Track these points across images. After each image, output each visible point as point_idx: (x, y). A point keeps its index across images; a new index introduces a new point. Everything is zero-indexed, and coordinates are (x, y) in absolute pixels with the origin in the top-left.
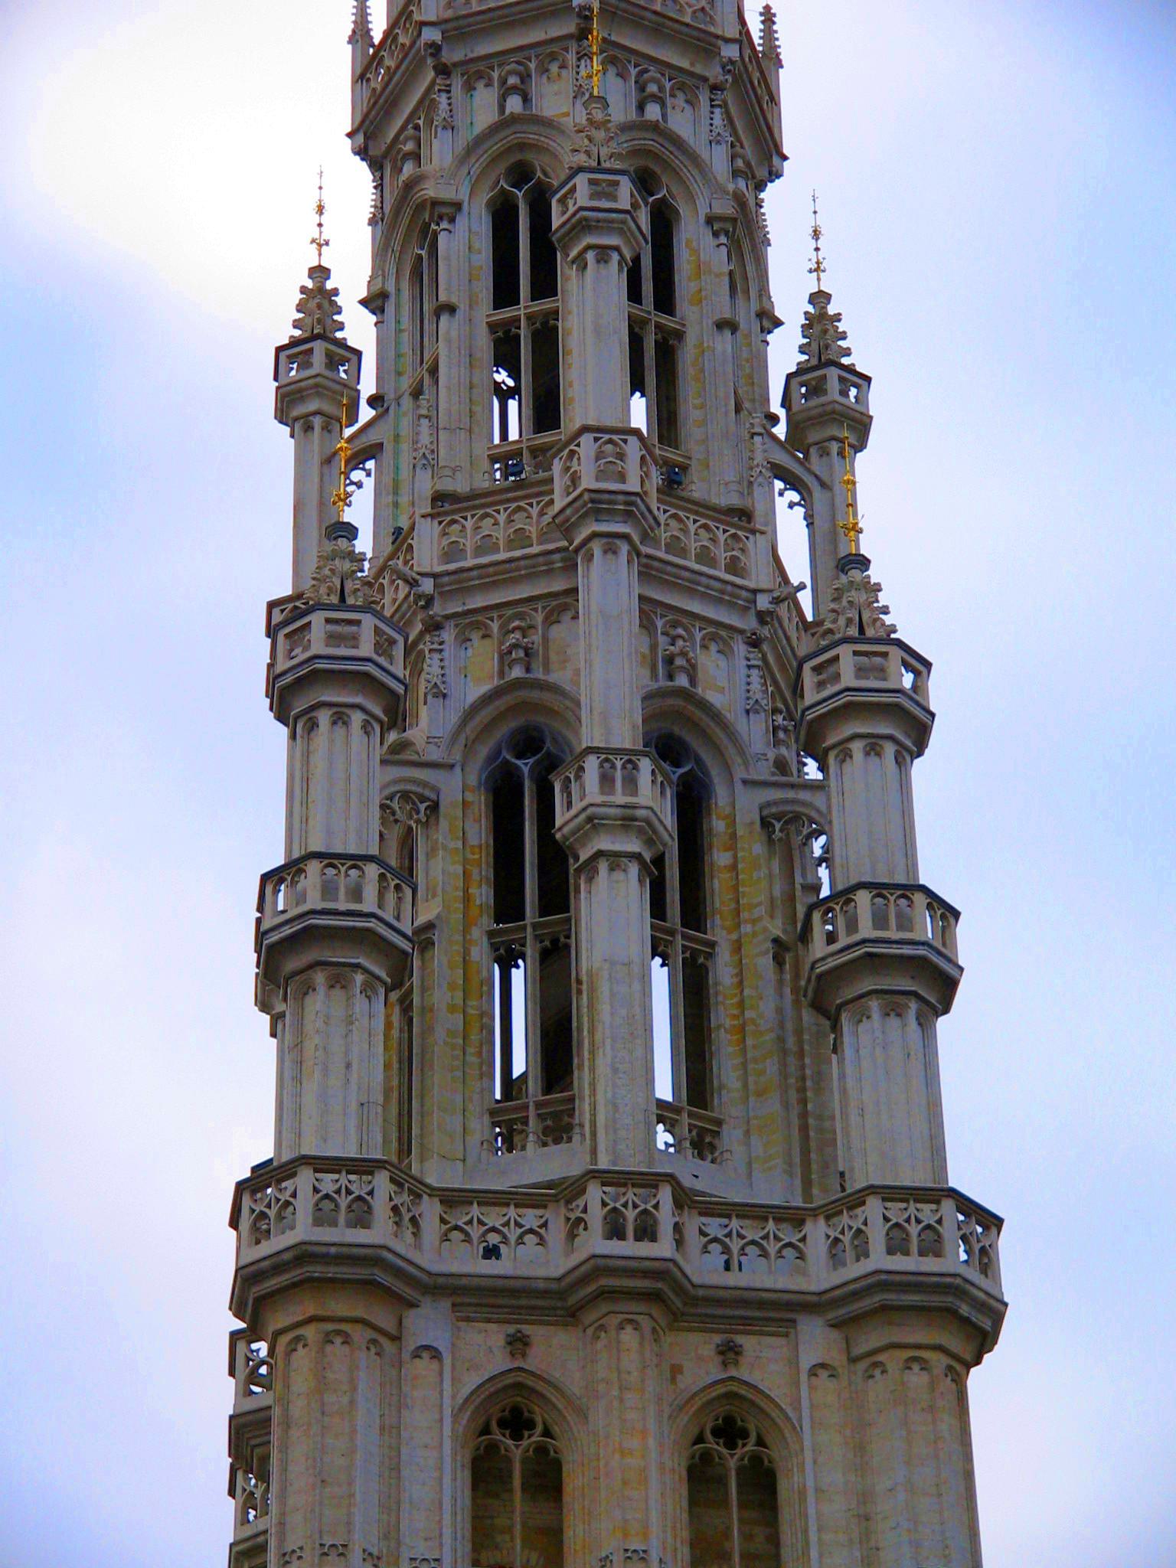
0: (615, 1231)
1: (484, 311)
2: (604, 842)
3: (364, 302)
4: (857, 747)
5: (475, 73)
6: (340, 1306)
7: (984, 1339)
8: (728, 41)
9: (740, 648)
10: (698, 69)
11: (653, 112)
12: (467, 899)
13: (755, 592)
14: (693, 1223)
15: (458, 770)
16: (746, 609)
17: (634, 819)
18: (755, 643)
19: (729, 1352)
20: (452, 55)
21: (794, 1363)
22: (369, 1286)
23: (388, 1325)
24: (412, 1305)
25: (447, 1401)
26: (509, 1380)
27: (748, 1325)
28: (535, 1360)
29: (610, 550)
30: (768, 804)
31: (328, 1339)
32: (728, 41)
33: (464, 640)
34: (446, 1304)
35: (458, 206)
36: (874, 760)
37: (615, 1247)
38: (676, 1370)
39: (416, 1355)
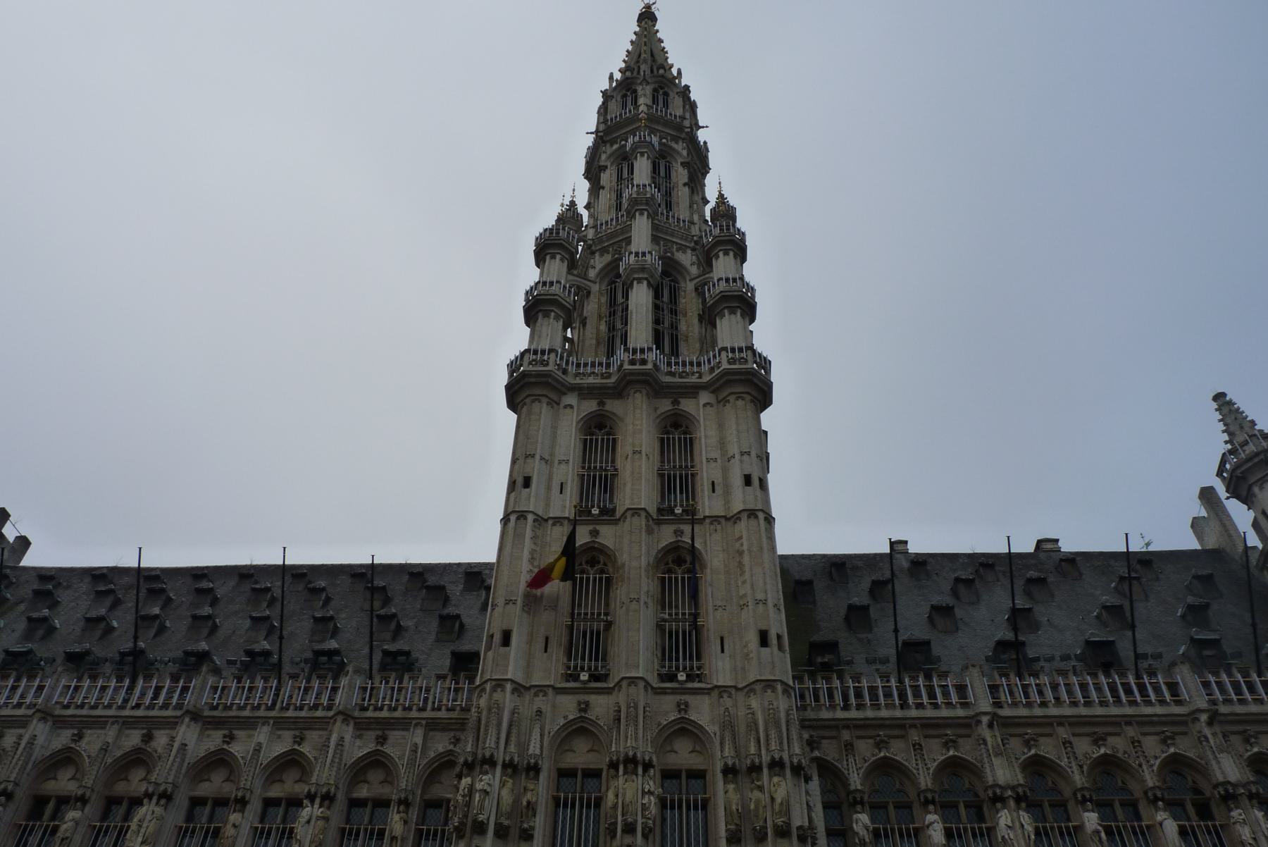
2: (636, 276)
3: (585, 207)
4: (721, 254)
6: (538, 391)
7: (763, 397)
8: (687, 128)
9: (689, 251)
10: (678, 135)
11: (664, 141)
13: (693, 236)
15: (598, 284)
16: (691, 241)
17: (645, 268)
18: (693, 249)
19: (676, 402)
21: (698, 405)
22: (547, 385)
23: (555, 398)
24: (565, 394)
25: (575, 418)
26: (598, 412)
29: (642, 214)
30: (697, 283)
31: (533, 401)
32: (687, 128)
33: (602, 255)
34: (576, 393)
35: (606, 167)
36: (726, 257)
38: (656, 409)
39: (565, 407)
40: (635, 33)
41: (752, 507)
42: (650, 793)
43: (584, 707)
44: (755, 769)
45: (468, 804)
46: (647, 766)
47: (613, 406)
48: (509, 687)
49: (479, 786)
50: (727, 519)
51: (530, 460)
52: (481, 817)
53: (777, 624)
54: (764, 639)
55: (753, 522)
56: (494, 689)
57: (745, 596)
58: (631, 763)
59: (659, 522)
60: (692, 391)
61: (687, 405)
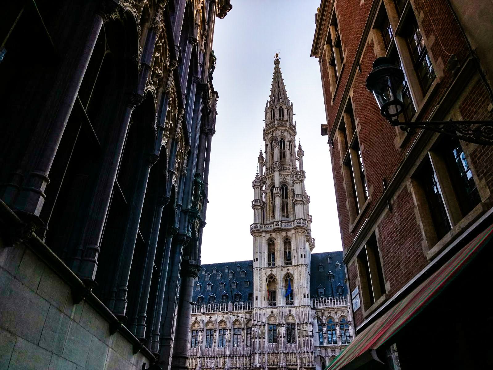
0: (276, 225)
1: (271, 152)
5: (269, 133)
9: (290, 176)
12: (269, 200)
14: (283, 224)
18: (291, 175)
19: (287, 233)
20: (267, 132)
23: (261, 235)
27: (288, 231)
28: (272, 236)
33: (269, 179)
37: (276, 227)
40: (273, 79)
41: (302, 263)
42: (284, 330)
43: (272, 312)
44: (302, 324)
45: (254, 333)
46: (284, 324)
47: (274, 235)
48: (258, 309)
49: (255, 330)
50: (298, 265)
51: (257, 253)
52: (256, 336)
53: (307, 292)
54: (305, 297)
55: (302, 267)
56: (256, 310)
57: (301, 285)
58: (280, 325)
59: (284, 267)
60: (290, 230)
61: (290, 234)
